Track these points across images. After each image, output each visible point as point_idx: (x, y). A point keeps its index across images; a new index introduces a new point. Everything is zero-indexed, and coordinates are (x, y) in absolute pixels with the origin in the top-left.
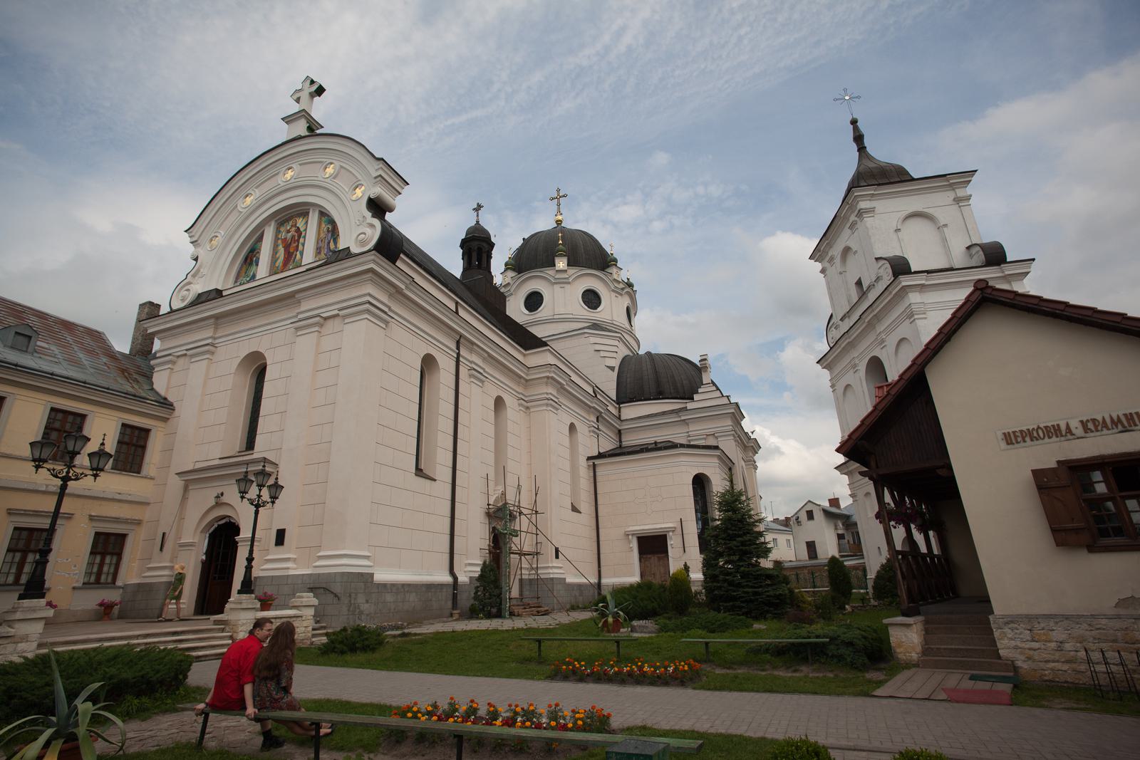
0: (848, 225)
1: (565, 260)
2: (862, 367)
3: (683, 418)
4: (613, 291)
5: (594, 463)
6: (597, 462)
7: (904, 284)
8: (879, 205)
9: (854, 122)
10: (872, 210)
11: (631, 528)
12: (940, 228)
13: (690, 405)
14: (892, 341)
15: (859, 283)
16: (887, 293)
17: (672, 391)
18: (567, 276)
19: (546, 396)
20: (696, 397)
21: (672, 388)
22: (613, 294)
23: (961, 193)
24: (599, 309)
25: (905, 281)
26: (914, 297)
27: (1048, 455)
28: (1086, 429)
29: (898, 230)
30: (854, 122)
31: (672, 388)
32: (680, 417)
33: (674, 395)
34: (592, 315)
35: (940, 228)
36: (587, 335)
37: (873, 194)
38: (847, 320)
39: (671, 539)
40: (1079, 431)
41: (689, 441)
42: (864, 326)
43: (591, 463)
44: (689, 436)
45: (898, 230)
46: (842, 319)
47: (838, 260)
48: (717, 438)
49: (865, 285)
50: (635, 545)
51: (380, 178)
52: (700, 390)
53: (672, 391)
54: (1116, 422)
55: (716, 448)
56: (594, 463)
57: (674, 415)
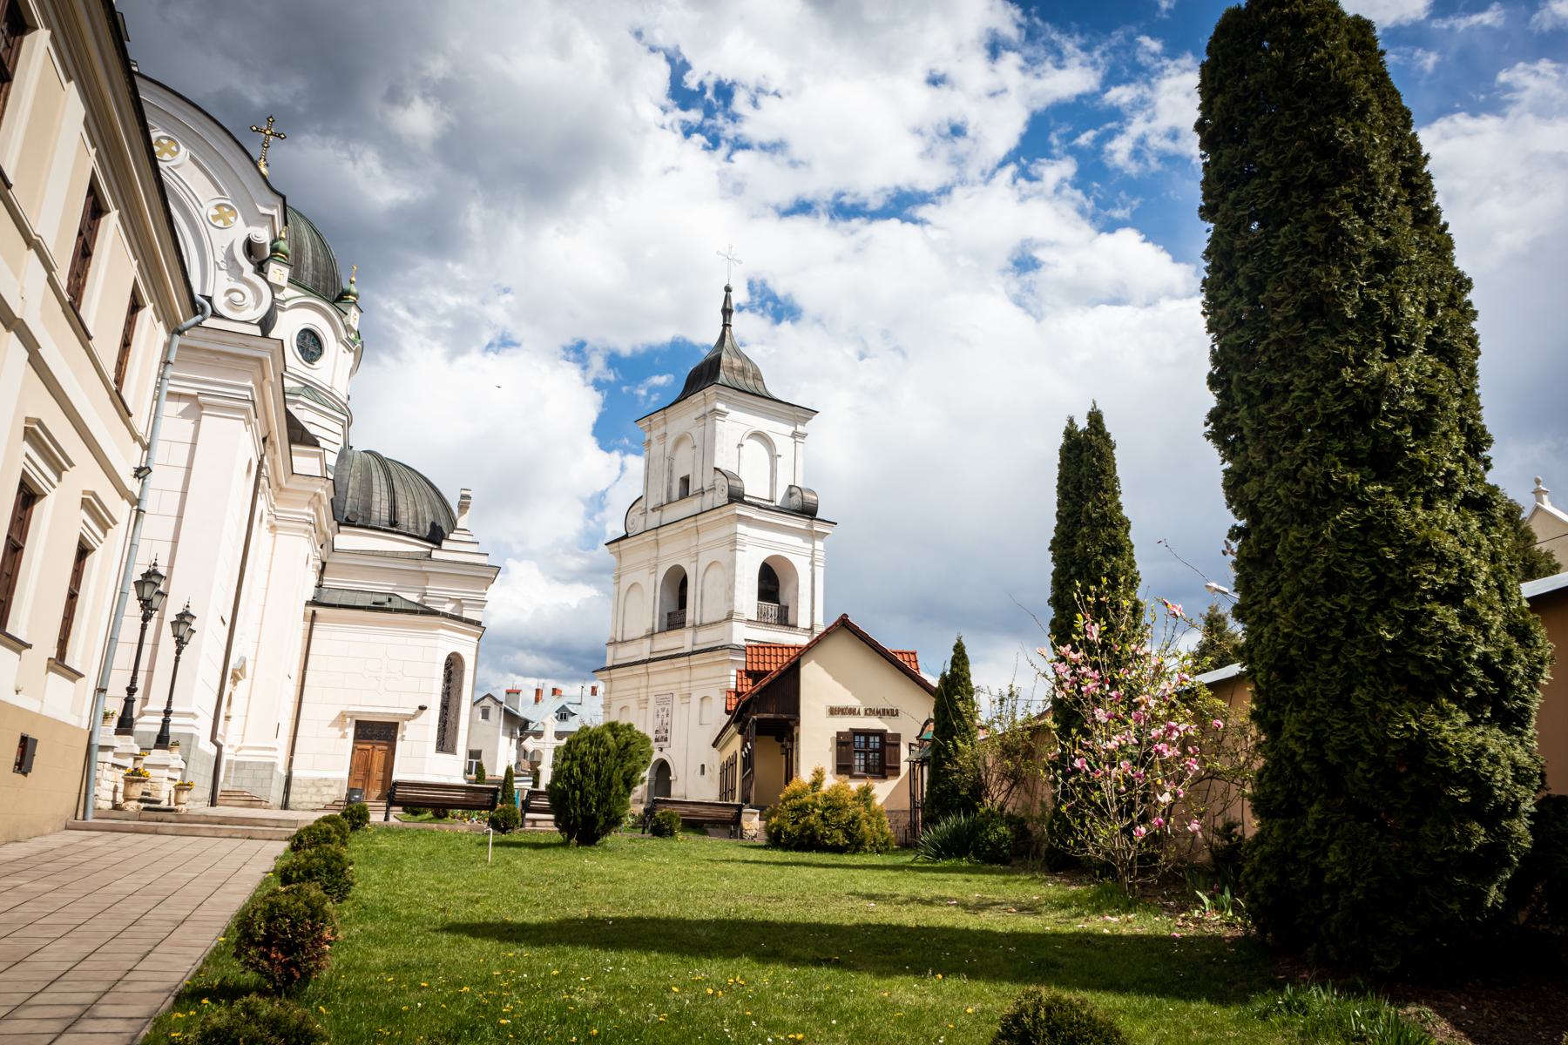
0: (697, 415)
1: (286, 271)
2: (662, 571)
3: (424, 569)
4: (343, 343)
5: (314, 612)
6: (319, 610)
7: (738, 512)
8: (734, 415)
9: (728, 289)
10: (724, 414)
11: (352, 709)
12: (774, 457)
13: (436, 554)
14: (705, 560)
15: (685, 481)
16: (717, 511)
17: (411, 525)
18: (283, 299)
19: (306, 517)
20: (445, 544)
21: (411, 520)
22: (342, 347)
23: (800, 429)
24: (317, 364)
25: (740, 510)
26: (741, 528)
27: (846, 724)
28: (866, 714)
29: (740, 445)
30: (728, 289)
31: (411, 520)
32: (421, 566)
33: (412, 532)
34: (305, 369)
35: (774, 457)
36: (299, 406)
37: (730, 398)
38: (658, 513)
39: (405, 728)
40: (862, 713)
41: (425, 601)
42: (679, 530)
43: (310, 609)
44: (425, 595)
45: (740, 445)
46: (653, 510)
47: (670, 441)
48: (462, 605)
49: (694, 486)
50: (351, 731)
51: (270, 219)
52: (452, 536)
53: (411, 525)
54: (878, 712)
55: (478, 624)
56: (314, 612)
57: (414, 562)
